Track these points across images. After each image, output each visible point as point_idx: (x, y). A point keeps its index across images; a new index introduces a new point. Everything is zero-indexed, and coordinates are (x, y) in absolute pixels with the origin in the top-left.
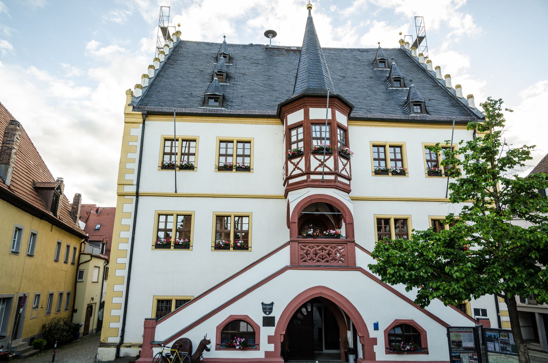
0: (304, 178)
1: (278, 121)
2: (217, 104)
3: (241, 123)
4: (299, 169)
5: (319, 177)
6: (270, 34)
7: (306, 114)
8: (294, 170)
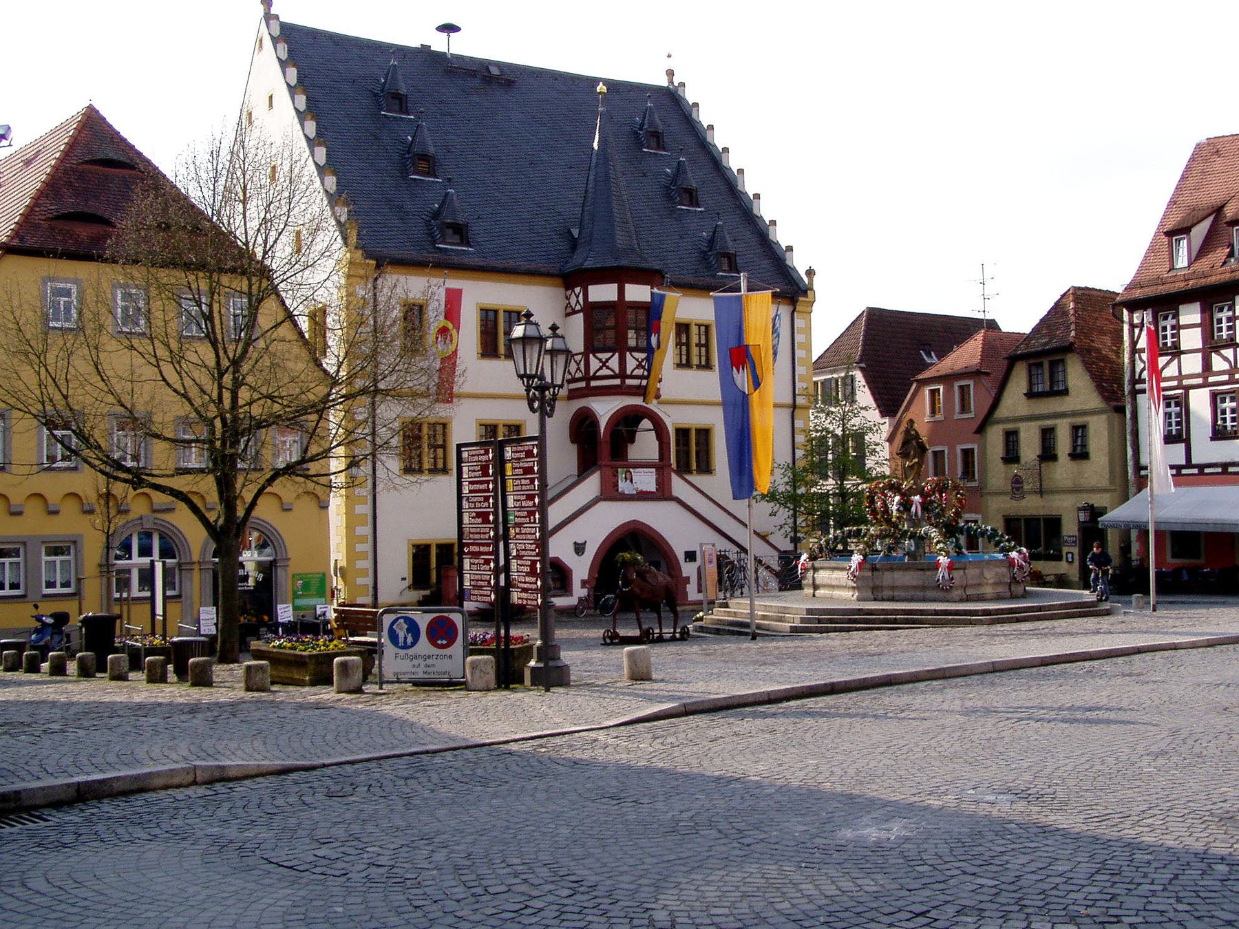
0: (617, 382)
1: (560, 281)
2: (457, 239)
3: (509, 282)
4: (608, 368)
5: (635, 382)
6: (449, 28)
7: (621, 292)
8: (601, 368)
